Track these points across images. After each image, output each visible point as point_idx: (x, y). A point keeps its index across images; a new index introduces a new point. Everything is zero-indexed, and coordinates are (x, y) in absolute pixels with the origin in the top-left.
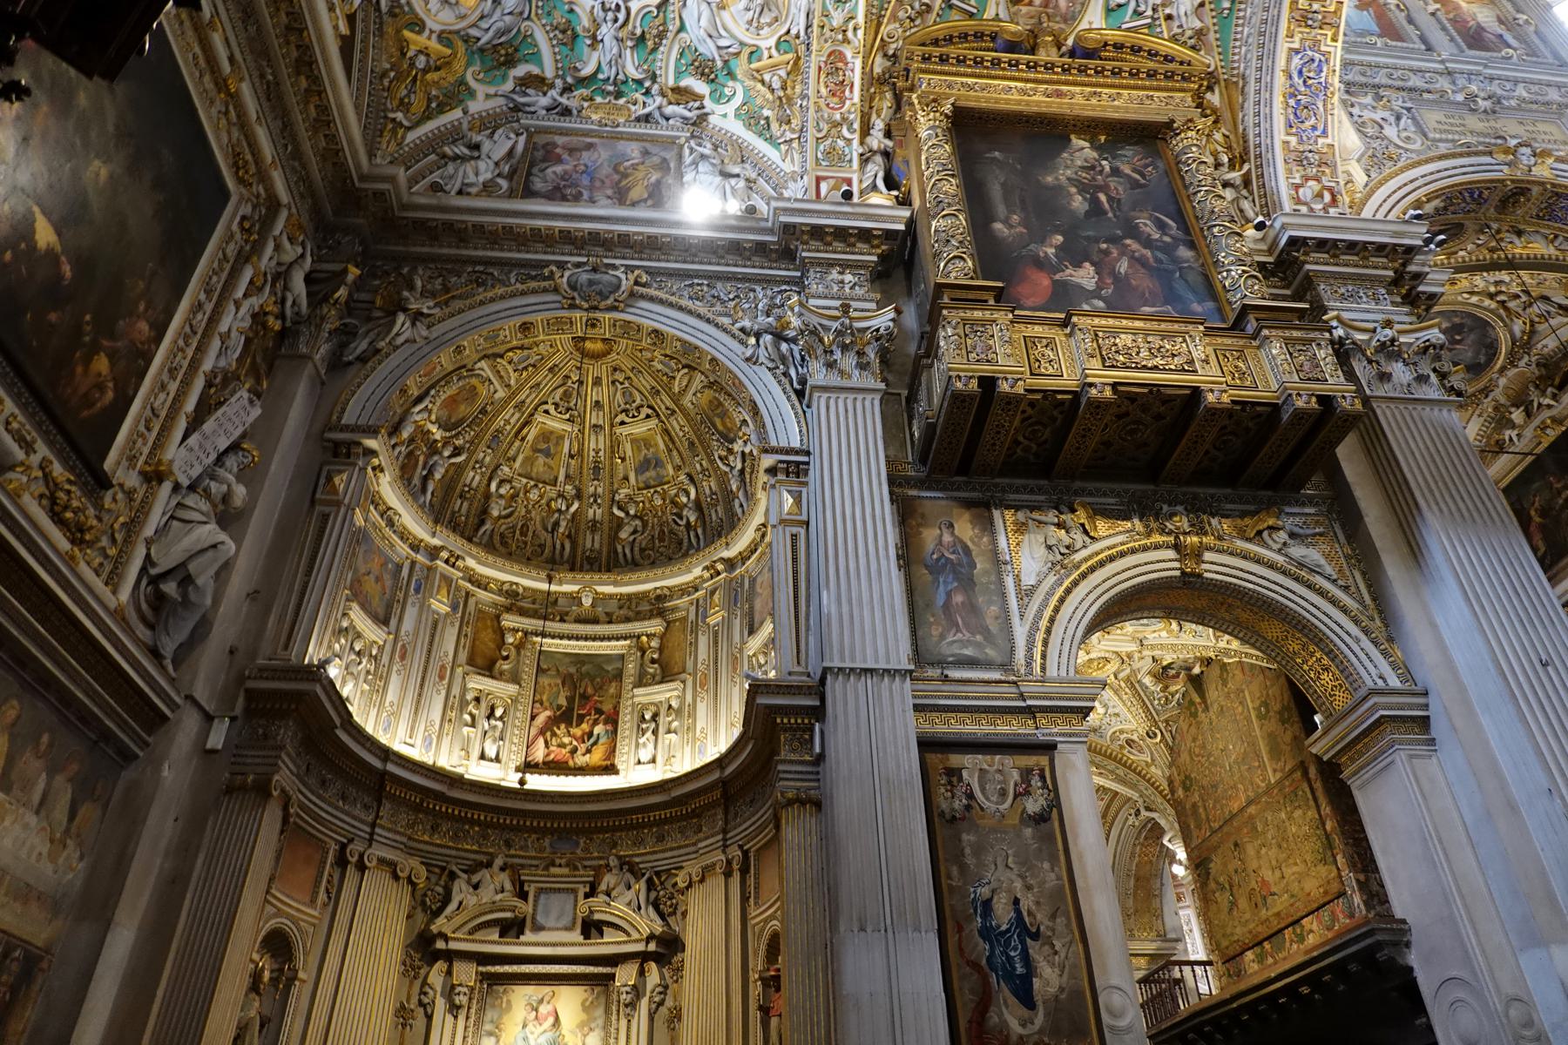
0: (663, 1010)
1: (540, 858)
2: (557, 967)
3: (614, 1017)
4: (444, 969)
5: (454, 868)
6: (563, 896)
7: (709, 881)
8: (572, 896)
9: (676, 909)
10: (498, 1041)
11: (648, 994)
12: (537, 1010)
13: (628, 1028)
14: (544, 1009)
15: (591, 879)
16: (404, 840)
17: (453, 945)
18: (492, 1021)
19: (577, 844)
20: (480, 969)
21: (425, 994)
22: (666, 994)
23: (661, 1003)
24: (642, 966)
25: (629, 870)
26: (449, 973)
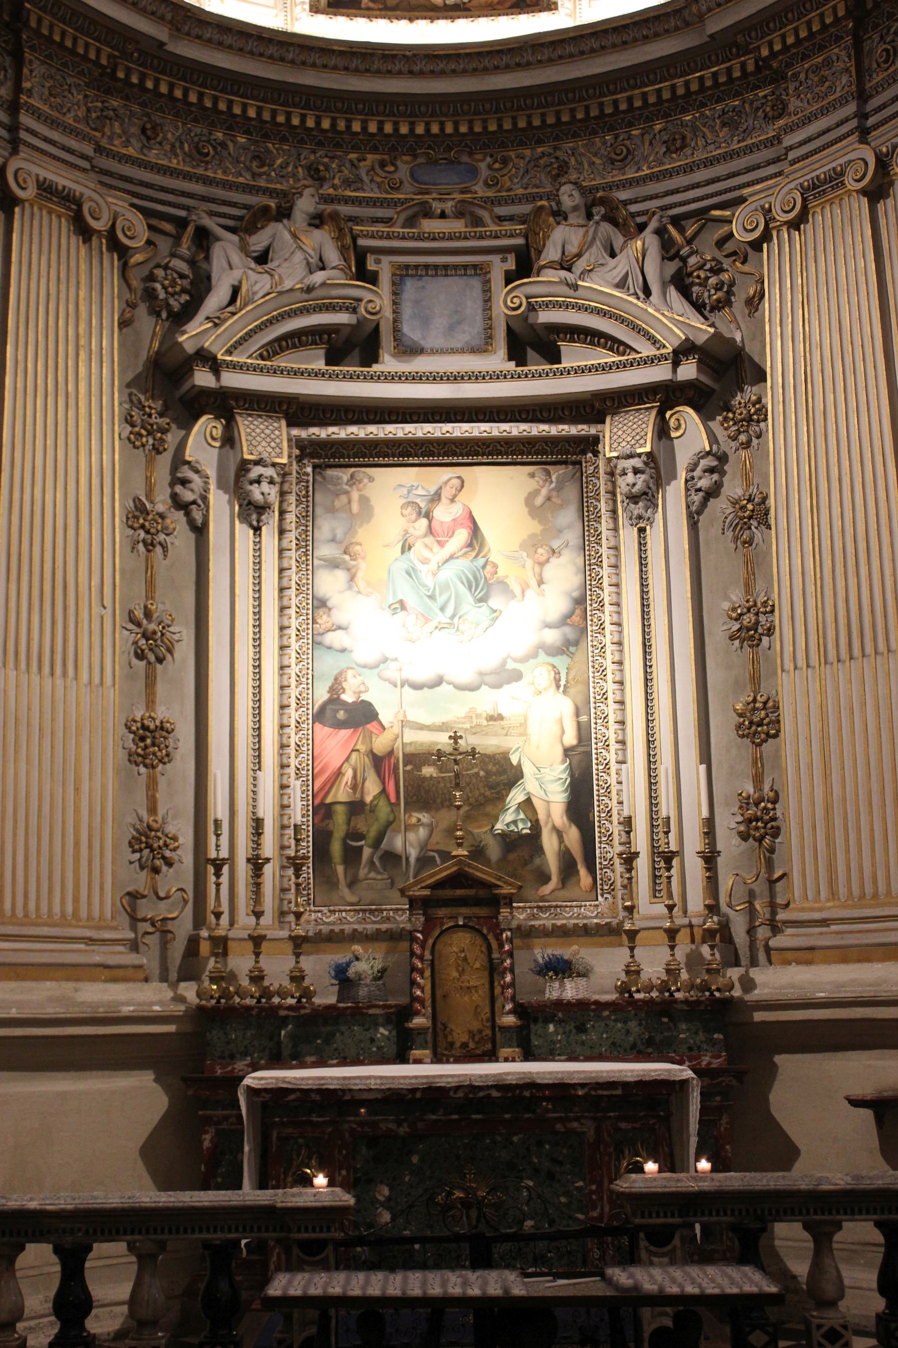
0: (720, 506)
1: (394, 203)
2: (466, 426)
3: (605, 524)
4: (218, 432)
5: (208, 222)
6: (454, 284)
7: (819, 219)
8: (476, 283)
9: (729, 293)
10: (352, 578)
11: (682, 475)
12: (428, 515)
13: (642, 545)
14: (444, 513)
15: (520, 241)
16: (89, 150)
17: (232, 380)
18: (333, 540)
19: (474, 172)
20: (295, 432)
21: (184, 482)
22: (723, 473)
23: (712, 493)
24: (661, 414)
25: (606, 218)
26: (229, 440)
